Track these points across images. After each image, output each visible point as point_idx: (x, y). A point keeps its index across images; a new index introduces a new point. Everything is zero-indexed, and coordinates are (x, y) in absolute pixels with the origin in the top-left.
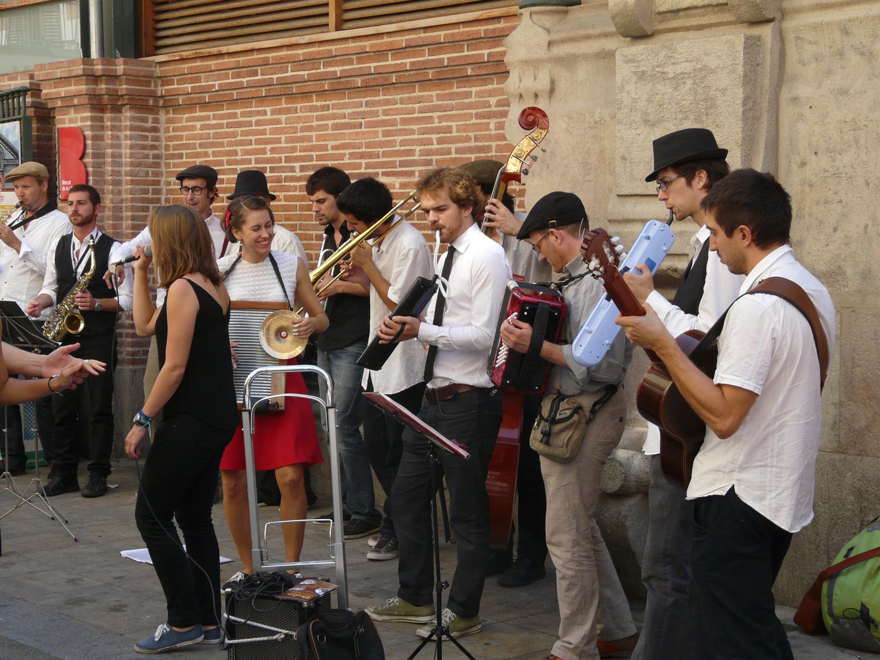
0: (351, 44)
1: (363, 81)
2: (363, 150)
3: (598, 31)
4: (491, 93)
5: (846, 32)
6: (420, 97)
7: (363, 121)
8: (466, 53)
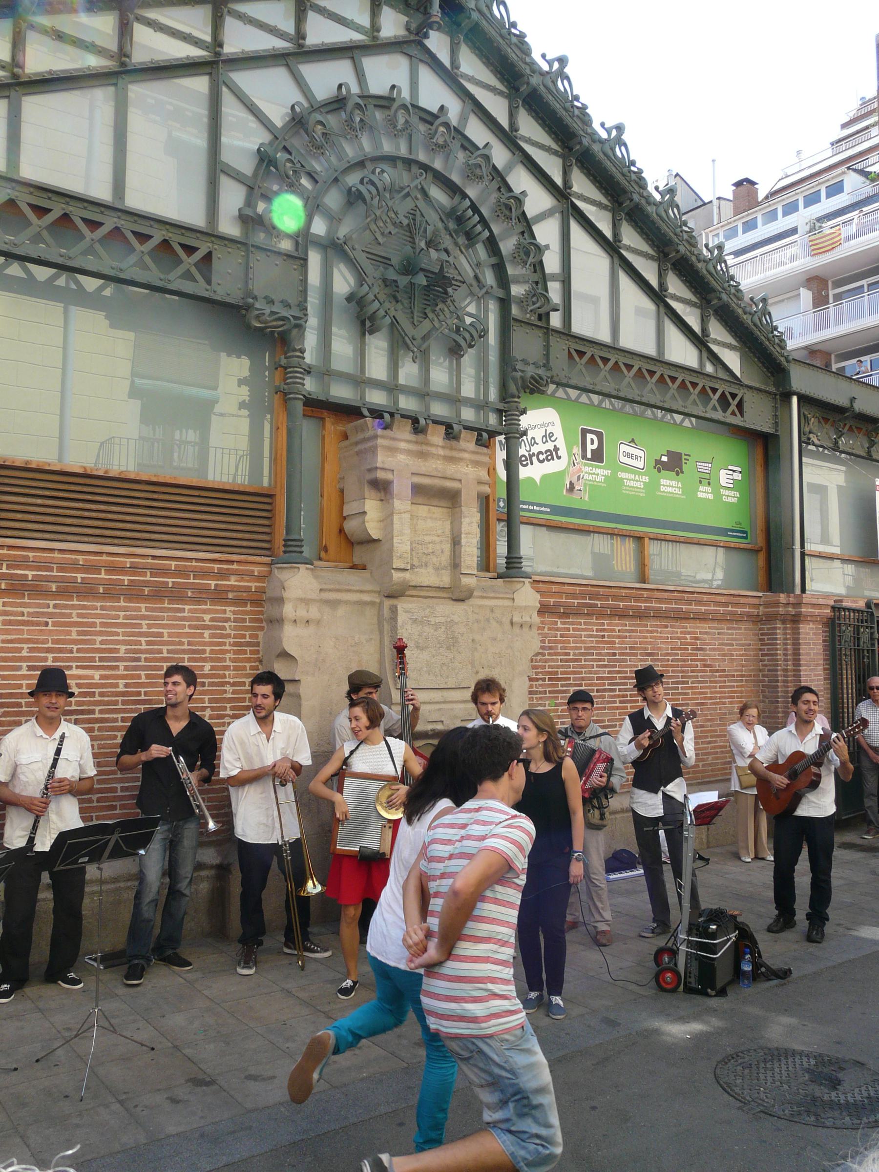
0: (56, 555)
1: (58, 587)
2: (50, 645)
3: (358, 588)
4: (205, 612)
5: (492, 611)
6: (127, 607)
7: (50, 621)
8: (192, 581)
